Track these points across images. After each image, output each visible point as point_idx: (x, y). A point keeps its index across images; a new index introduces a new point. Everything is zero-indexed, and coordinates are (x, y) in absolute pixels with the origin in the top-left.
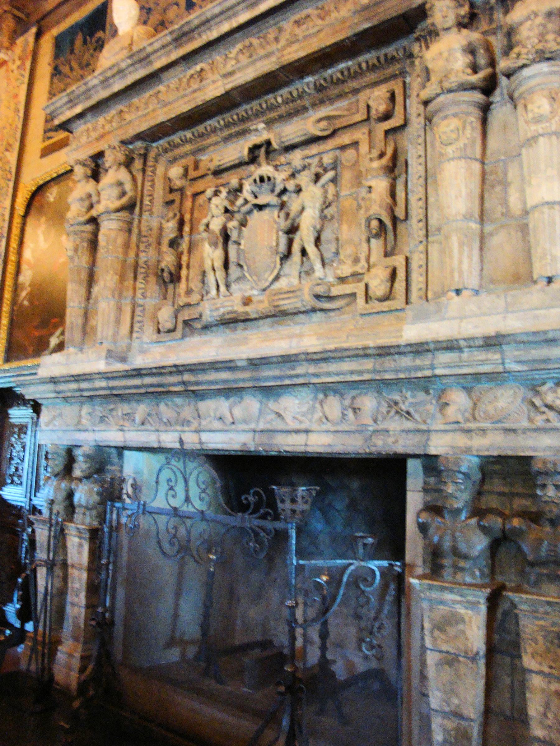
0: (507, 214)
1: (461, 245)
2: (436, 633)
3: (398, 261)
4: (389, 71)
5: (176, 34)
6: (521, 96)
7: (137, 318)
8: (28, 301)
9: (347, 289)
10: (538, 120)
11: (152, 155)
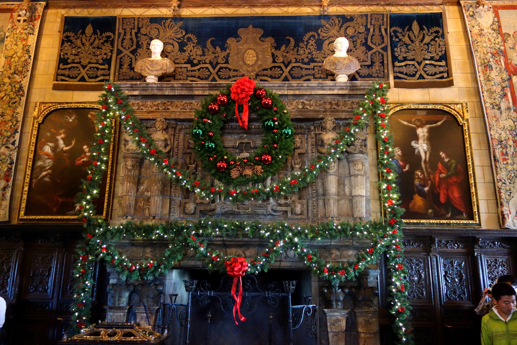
0: (344, 194)
1: (334, 203)
2: (332, 326)
3: (305, 201)
4: (300, 131)
5: (211, 85)
6: (353, 161)
7: (172, 206)
8: (50, 178)
9: (284, 209)
10: (359, 170)
11: (178, 127)
